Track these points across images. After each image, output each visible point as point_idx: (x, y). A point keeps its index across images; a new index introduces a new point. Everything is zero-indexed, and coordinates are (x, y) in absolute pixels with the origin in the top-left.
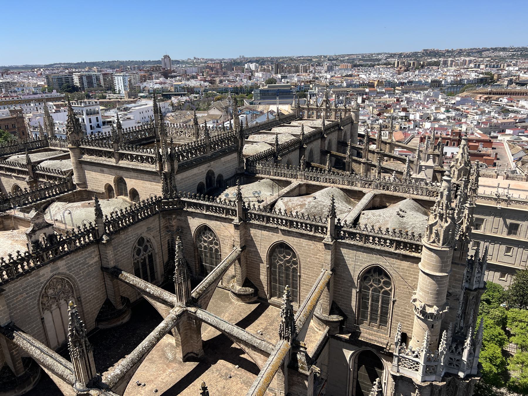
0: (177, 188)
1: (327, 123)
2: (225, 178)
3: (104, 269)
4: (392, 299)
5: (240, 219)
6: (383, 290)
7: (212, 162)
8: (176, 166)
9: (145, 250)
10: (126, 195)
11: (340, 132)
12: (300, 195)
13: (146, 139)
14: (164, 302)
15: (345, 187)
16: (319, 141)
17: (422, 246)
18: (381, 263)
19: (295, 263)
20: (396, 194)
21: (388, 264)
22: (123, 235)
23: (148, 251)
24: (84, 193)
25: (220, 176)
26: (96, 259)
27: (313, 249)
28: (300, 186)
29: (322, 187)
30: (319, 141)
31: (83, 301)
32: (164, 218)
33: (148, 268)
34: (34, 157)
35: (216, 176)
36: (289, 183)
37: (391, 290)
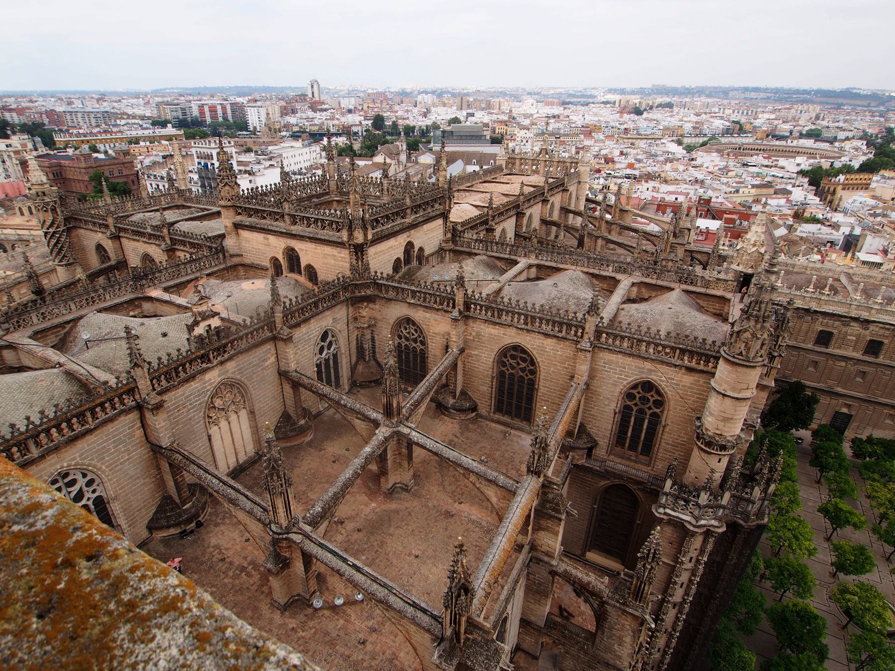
0: (371, 266)
1: (551, 180)
2: (427, 252)
3: (283, 375)
4: (663, 423)
5: (460, 312)
6: (651, 411)
7: (412, 231)
8: (370, 237)
9: (329, 349)
10: (300, 273)
11: (565, 193)
12: (528, 280)
13: (318, 196)
14: (366, 418)
15: (591, 271)
16: (540, 204)
17: (717, 359)
18: (655, 378)
19: (533, 373)
20: (660, 283)
21: (663, 379)
22: (304, 329)
23: (332, 349)
24: (240, 268)
25: (421, 249)
26: (273, 359)
27: (560, 356)
28: (530, 266)
29: (558, 270)
30: (540, 204)
31: (257, 413)
32: (352, 305)
33: (332, 371)
34: (170, 216)
35: (416, 250)
36: (516, 263)
37: (662, 412)
